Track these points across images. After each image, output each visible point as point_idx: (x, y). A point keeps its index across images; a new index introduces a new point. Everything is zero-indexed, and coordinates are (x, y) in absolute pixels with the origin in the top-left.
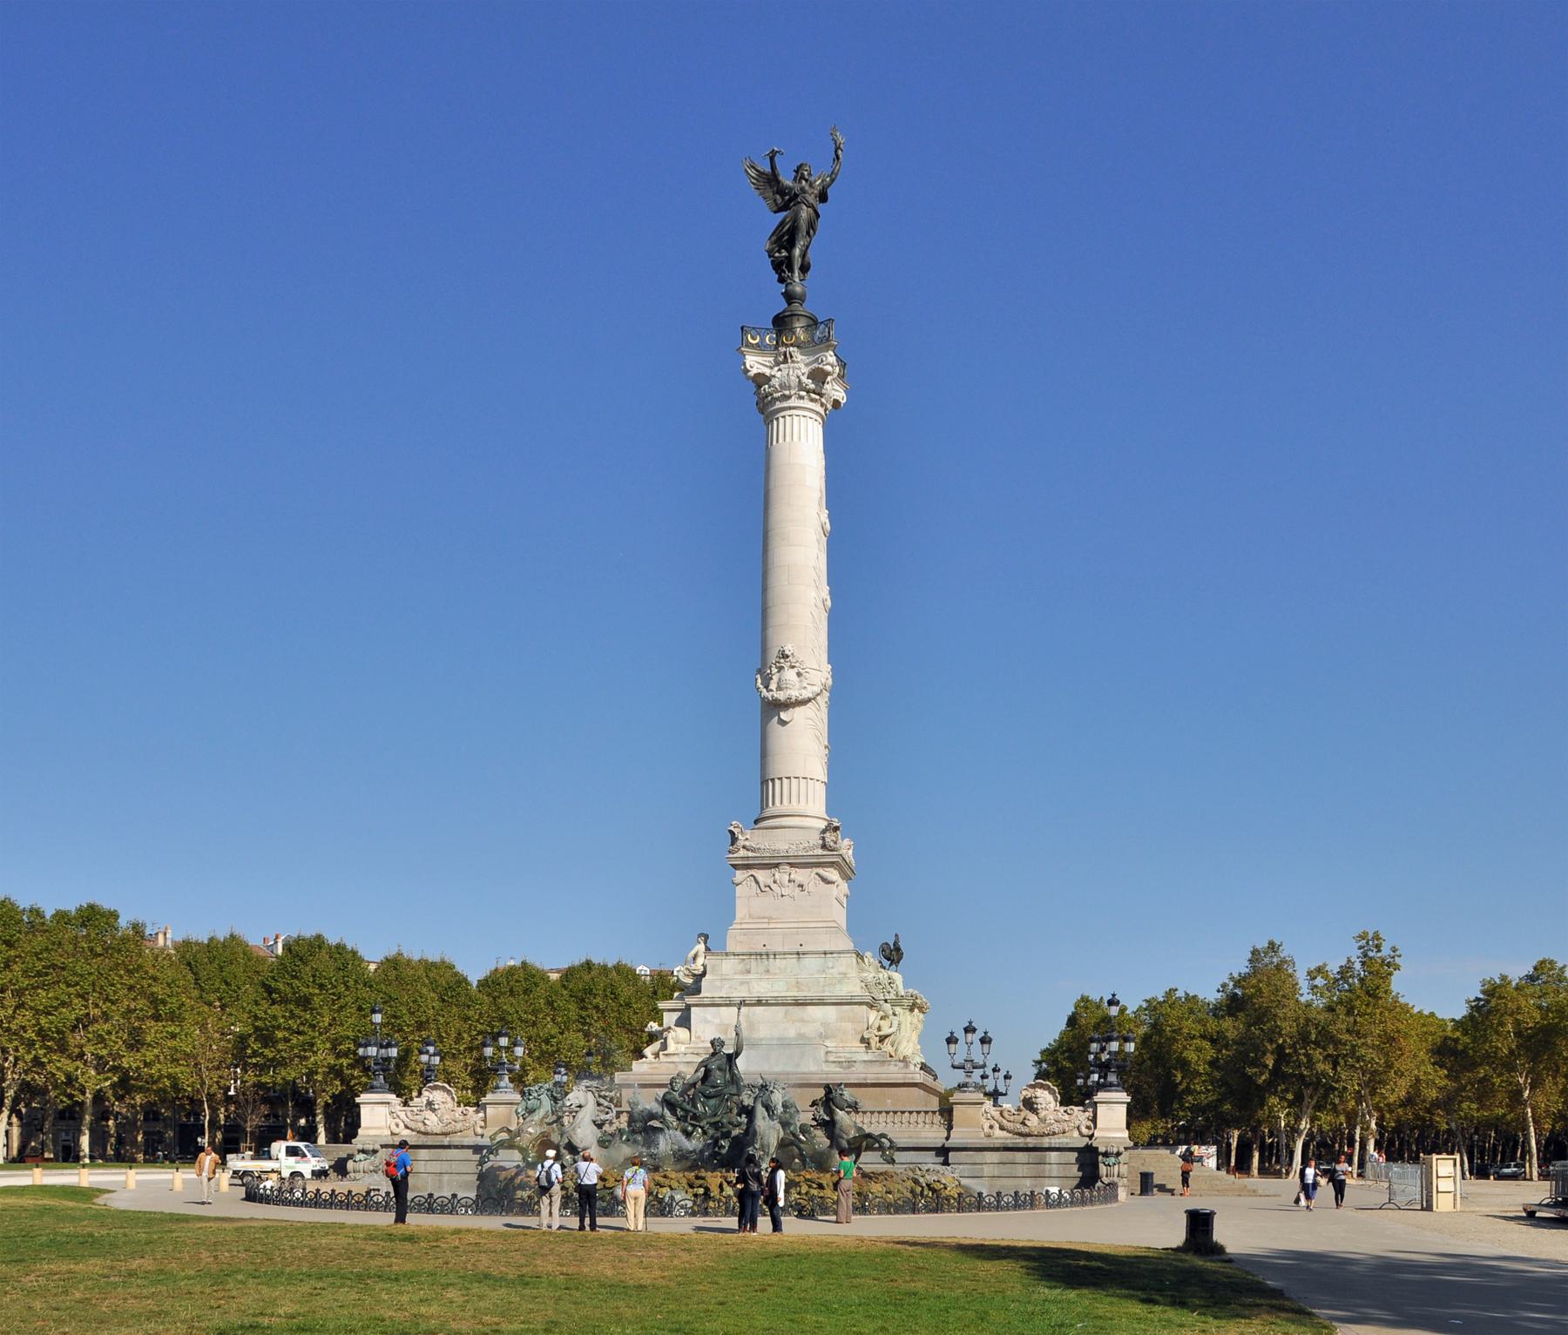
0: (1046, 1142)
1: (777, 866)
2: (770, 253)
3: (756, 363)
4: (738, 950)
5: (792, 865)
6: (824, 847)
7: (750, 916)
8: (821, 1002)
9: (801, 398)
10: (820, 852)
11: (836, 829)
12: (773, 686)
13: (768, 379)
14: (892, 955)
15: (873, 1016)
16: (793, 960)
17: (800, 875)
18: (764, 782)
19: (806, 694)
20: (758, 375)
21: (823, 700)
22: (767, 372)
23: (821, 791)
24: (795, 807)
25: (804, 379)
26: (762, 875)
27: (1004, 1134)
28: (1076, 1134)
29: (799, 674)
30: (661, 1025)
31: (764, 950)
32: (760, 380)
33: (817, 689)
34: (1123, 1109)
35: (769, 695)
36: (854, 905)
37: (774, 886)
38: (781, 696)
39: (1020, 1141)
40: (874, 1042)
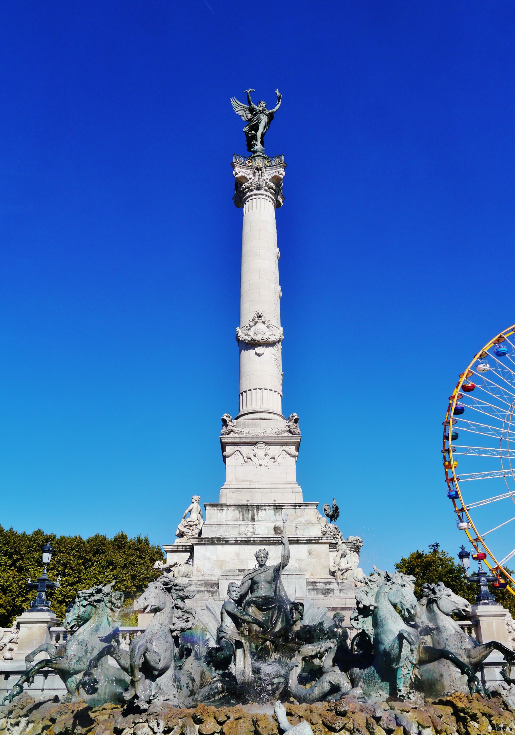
1: (255, 444)
3: (240, 171)
5: (266, 444)
6: (290, 431)
7: (236, 479)
9: (266, 191)
10: (286, 434)
12: (251, 333)
19: (272, 339)
20: (243, 177)
22: (248, 177)
25: (267, 181)
26: (246, 450)
30: (165, 563)
32: (242, 180)
36: (303, 476)
37: (253, 458)
40: (338, 573)
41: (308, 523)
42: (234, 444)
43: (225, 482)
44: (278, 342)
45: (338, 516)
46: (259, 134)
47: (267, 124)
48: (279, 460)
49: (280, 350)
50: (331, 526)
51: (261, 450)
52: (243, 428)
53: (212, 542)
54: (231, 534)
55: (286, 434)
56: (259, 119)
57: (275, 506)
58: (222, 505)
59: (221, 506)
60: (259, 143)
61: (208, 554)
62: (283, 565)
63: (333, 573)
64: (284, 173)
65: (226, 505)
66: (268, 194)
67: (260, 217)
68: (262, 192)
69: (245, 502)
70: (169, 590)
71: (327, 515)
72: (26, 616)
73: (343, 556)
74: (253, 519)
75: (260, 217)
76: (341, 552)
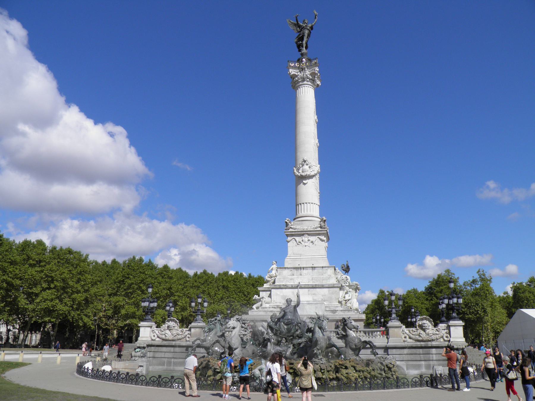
0: (430, 344)
1: (303, 235)
2: (296, 43)
3: (292, 72)
4: (289, 266)
5: (309, 235)
6: (321, 227)
7: (294, 254)
8: (322, 287)
9: (308, 81)
10: (319, 229)
11: (325, 221)
12: (300, 171)
13: (297, 76)
14: (346, 269)
15: (342, 293)
16: (310, 271)
17: (312, 238)
18: (297, 205)
19: (312, 174)
20: (294, 74)
21: (318, 176)
23: (317, 208)
24: (309, 213)
25: (308, 76)
26: (298, 239)
27: (411, 340)
28: (442, 340)
29: (310, 167)
30: (259, 296)
31: (299, 266)
33: (316, 172)
34: (461, 329)
35: (299, 174)
36: (330, 251)
38: (303, 174)
39: (419, 344)
40: (344, 302)
41: (330, 277)
42: (292, 235)
43: (287, 254)
44: (316, 174)
45: (349, 270)
46: (304, 42)
47: (309, 35)
48: (316, 243)
49: (318, 179)
50: (344, 276)
51: (305, 238)
52: (296, 226)
53: (280, 287)
54: (290, 283)
55: (319, 229)
56: (304, 33)
57: (312, 267)
58: (285, 268)
59: (285, 268)
60: (304, 49)
61: (278, 293)
62: (298, 304)
63: (340, 302)
64: (318, 70)
65: (288, 268)
66: (309, 83)
67: (307, 96)
68: (305, 82)
69: (297, 266)
70: (239, 321)
71: (343, 270)
72: (193, 324)
73: (346, 293)
74: (301, 275)
75: (307, 96)
76: (345, 291)
